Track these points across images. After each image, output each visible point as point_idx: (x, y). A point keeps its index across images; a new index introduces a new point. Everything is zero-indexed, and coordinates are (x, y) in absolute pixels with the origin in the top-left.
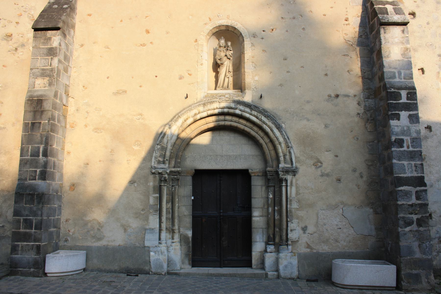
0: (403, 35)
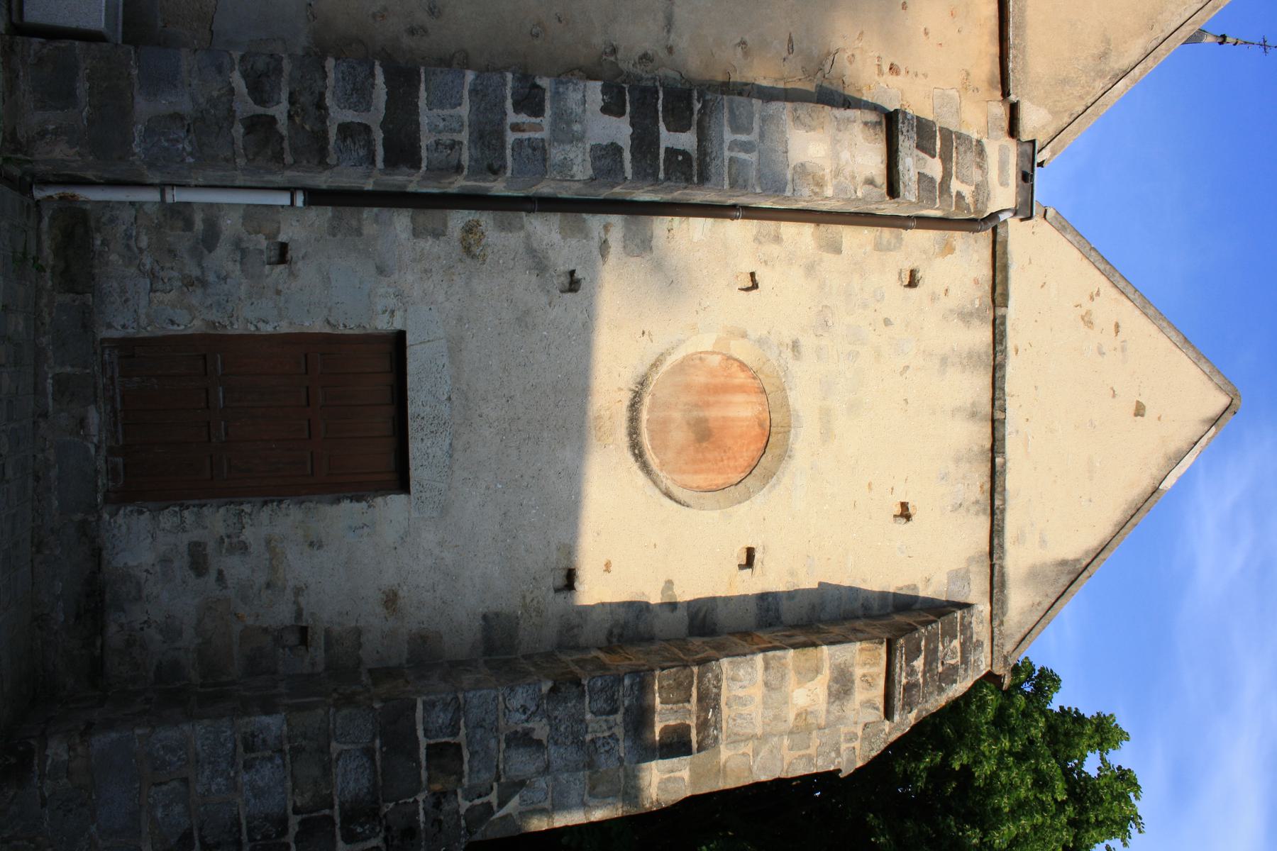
0: (860, 179)
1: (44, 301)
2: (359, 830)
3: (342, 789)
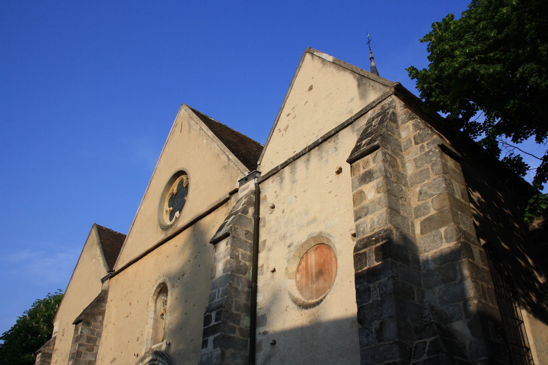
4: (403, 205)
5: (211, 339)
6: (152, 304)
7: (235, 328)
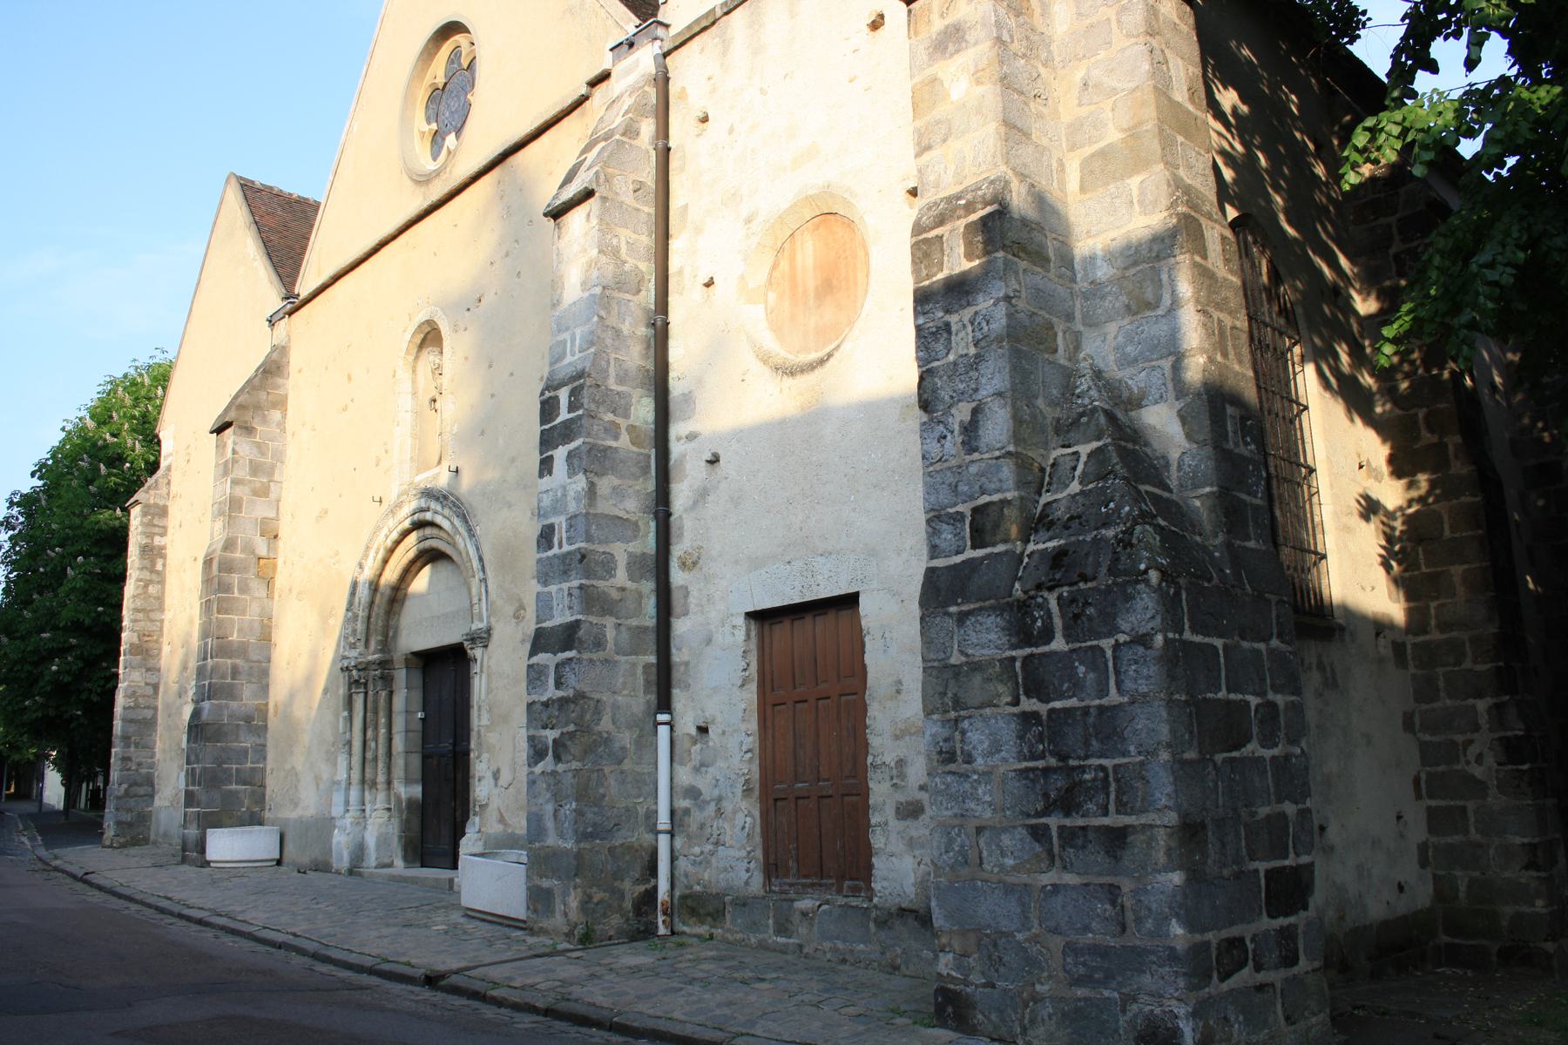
1: (729, 936)
2: (1039, 623)
3: (997, 647)
4: (1040, 116)
5: (560, 454)
6: (404, 375)
7: (618, 426)
